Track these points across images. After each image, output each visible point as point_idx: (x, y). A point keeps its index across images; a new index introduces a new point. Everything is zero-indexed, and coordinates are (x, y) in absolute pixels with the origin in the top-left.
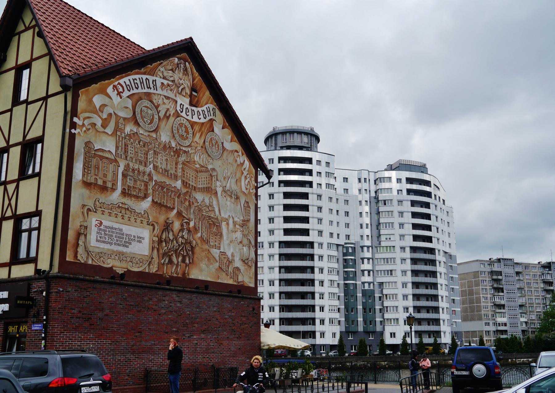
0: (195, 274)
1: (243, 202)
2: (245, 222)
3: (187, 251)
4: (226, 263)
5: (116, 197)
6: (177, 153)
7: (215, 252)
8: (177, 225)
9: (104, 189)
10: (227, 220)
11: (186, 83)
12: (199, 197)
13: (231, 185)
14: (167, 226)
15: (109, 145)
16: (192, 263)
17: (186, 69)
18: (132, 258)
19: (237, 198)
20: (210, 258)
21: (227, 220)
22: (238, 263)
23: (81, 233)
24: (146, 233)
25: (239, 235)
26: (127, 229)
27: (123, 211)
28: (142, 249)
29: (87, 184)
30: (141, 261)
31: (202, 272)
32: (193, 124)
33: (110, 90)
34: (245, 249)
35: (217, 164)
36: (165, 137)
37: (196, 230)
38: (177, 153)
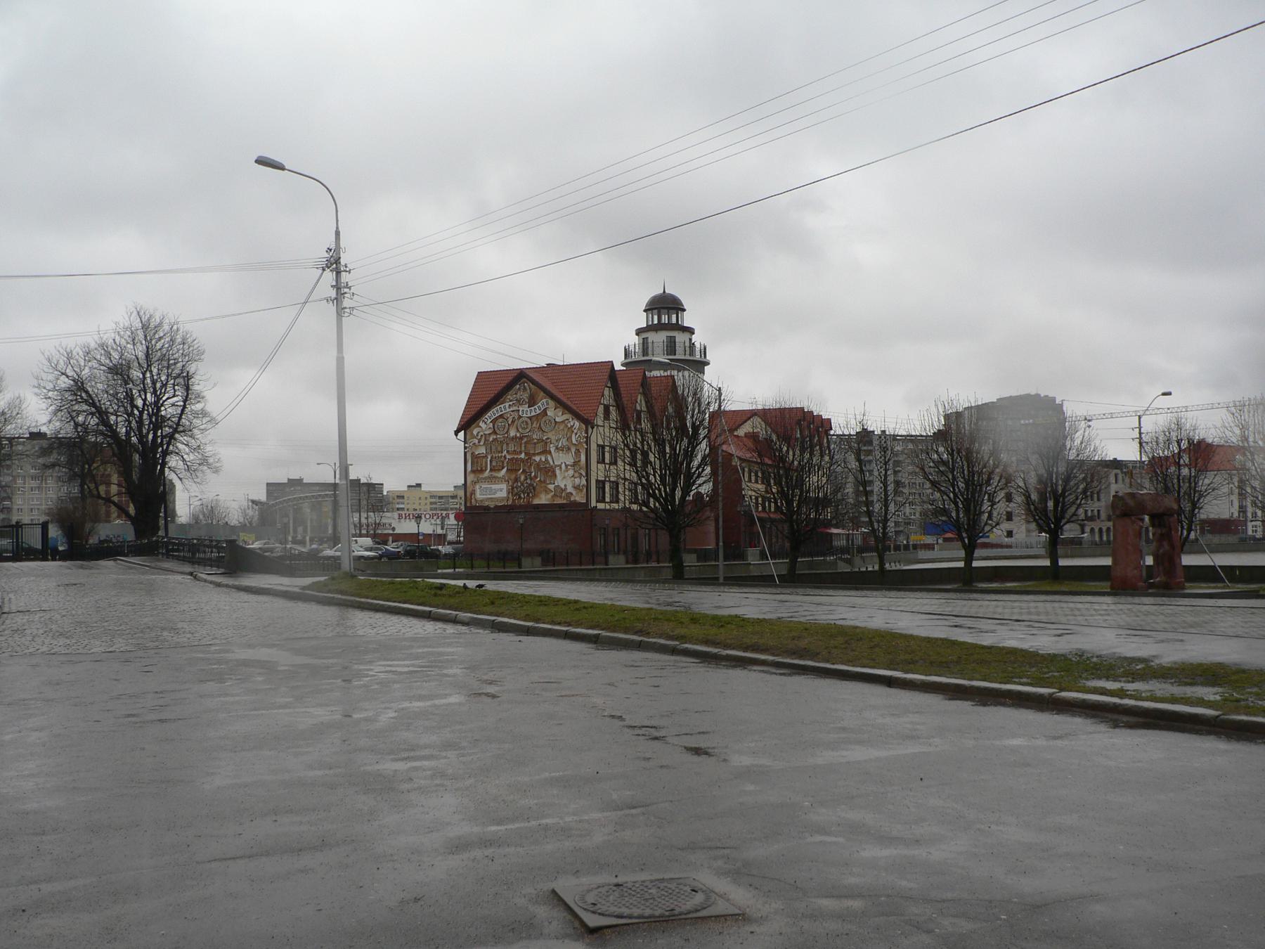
0: (536, 501)
1: (573, 450)
2: (576, 464)
3: (532, 490)
4: (560, 491)
5: (487, 473)
6: (521, 438)
7: (551, 487)
8: (523, 478)
9: (482, 471)
10: (560, 466)
11: (525, 396)
12: (537, 458)
13: (564, 442)
14: (516, 480)
15: (482, 450)
16: (534, 496)
17: (525, 389)
18: (497, 499)
19: (569, 449)
20: (547, 491)
21: (560, 466)
22: (570, 489)
23: (473, 493)
24: (504, 486)
25: (571, 472)
26: (494, 487)
27: (492, 479)
28: (504, 494)
29: (473, 471)
30: (502, 499)
31: (543, 499)
32: (530, 418)
33: (481, 424)
34: (577, 481)
35: (552, 436)
36: (512, 433)
37: (536, 477)
38: (521, 438)
